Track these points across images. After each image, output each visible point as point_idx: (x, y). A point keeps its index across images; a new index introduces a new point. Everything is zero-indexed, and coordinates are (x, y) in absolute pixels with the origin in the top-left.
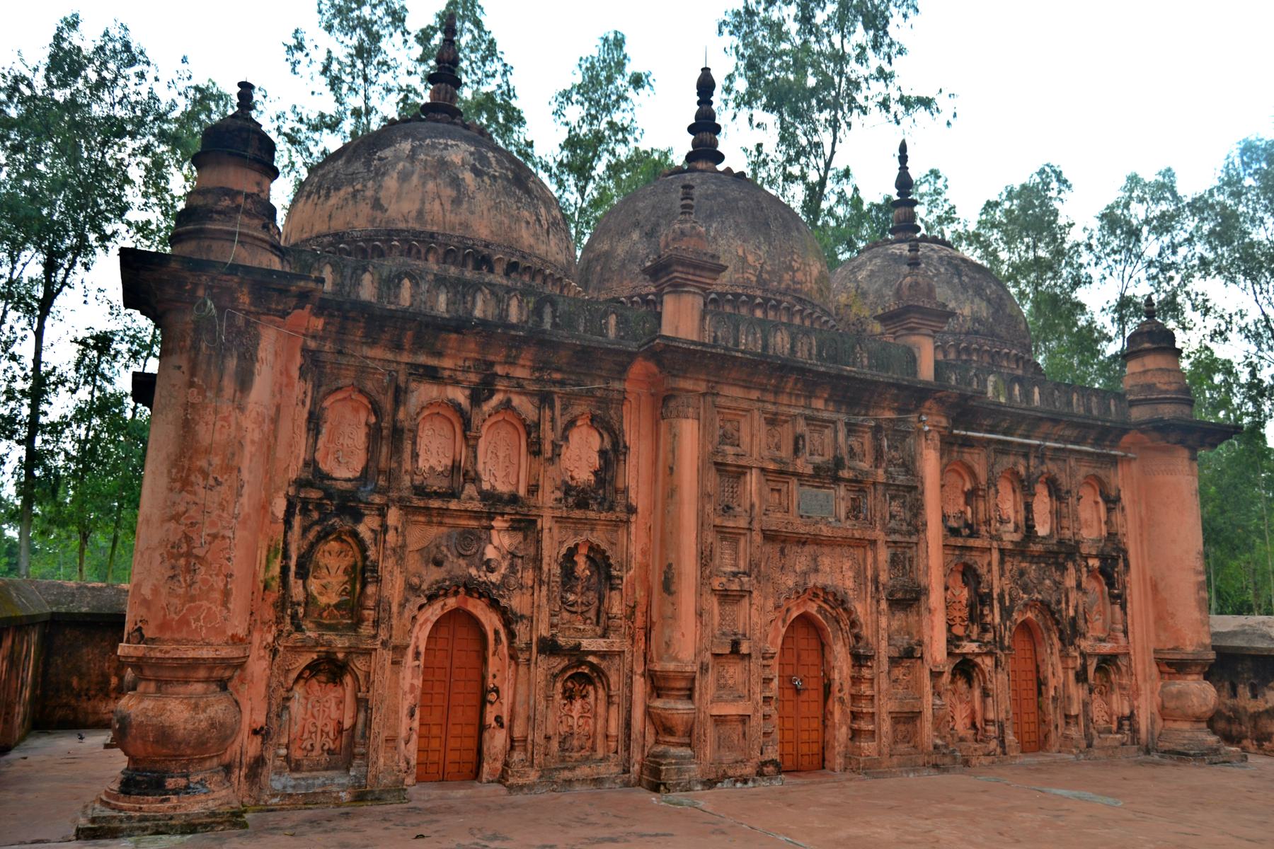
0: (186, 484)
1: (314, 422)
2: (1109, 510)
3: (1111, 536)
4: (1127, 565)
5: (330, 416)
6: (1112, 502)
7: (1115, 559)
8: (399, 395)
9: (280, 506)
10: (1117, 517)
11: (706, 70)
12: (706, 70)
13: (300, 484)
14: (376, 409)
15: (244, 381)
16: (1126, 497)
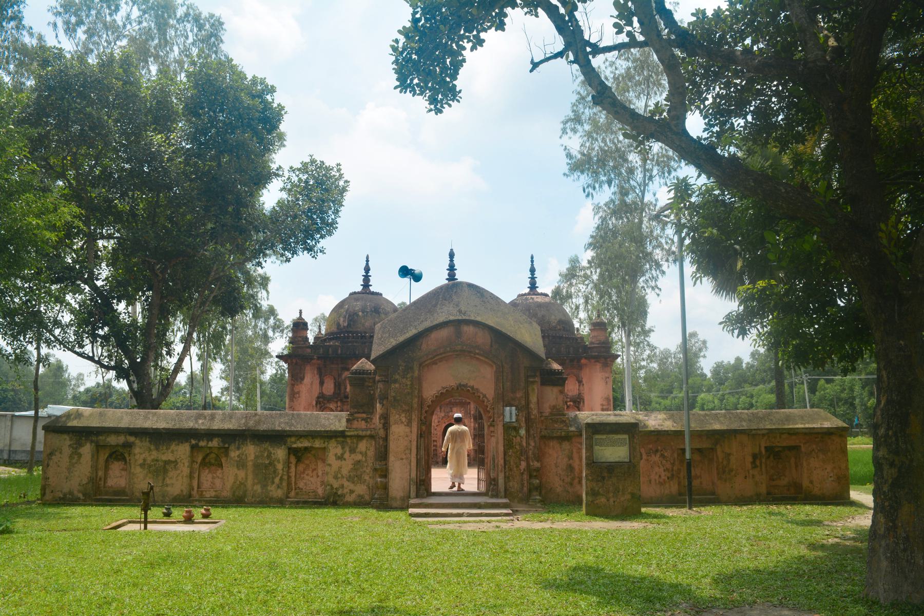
0: (293, 401)
1: (322, 383)
2: (579, 386)
3: (580, 394)
4: (583, 402)
5: (326, 381)
6: (580, 382)
7: (579, 402)
8: (340, 375)
9: (314, 403)
10: (581, 388)
11: (452, 250)
12: (452, 250)
13: (318, 398)
14: (335, 379)
15: (303, 379)
16: (584, 381)
